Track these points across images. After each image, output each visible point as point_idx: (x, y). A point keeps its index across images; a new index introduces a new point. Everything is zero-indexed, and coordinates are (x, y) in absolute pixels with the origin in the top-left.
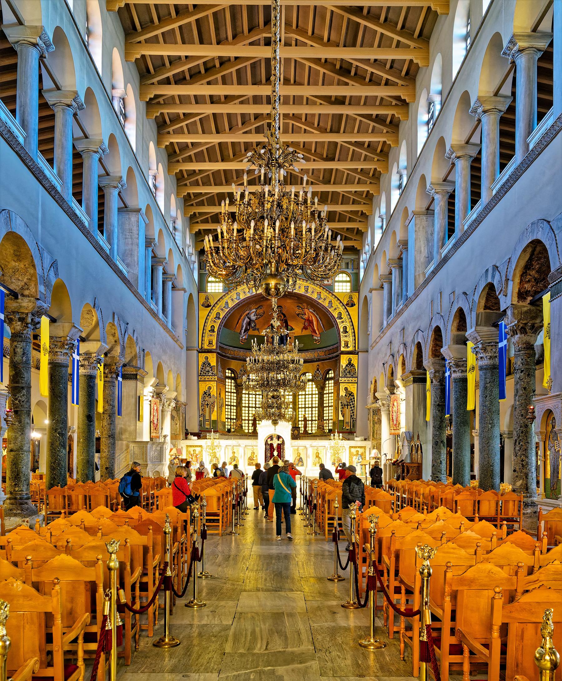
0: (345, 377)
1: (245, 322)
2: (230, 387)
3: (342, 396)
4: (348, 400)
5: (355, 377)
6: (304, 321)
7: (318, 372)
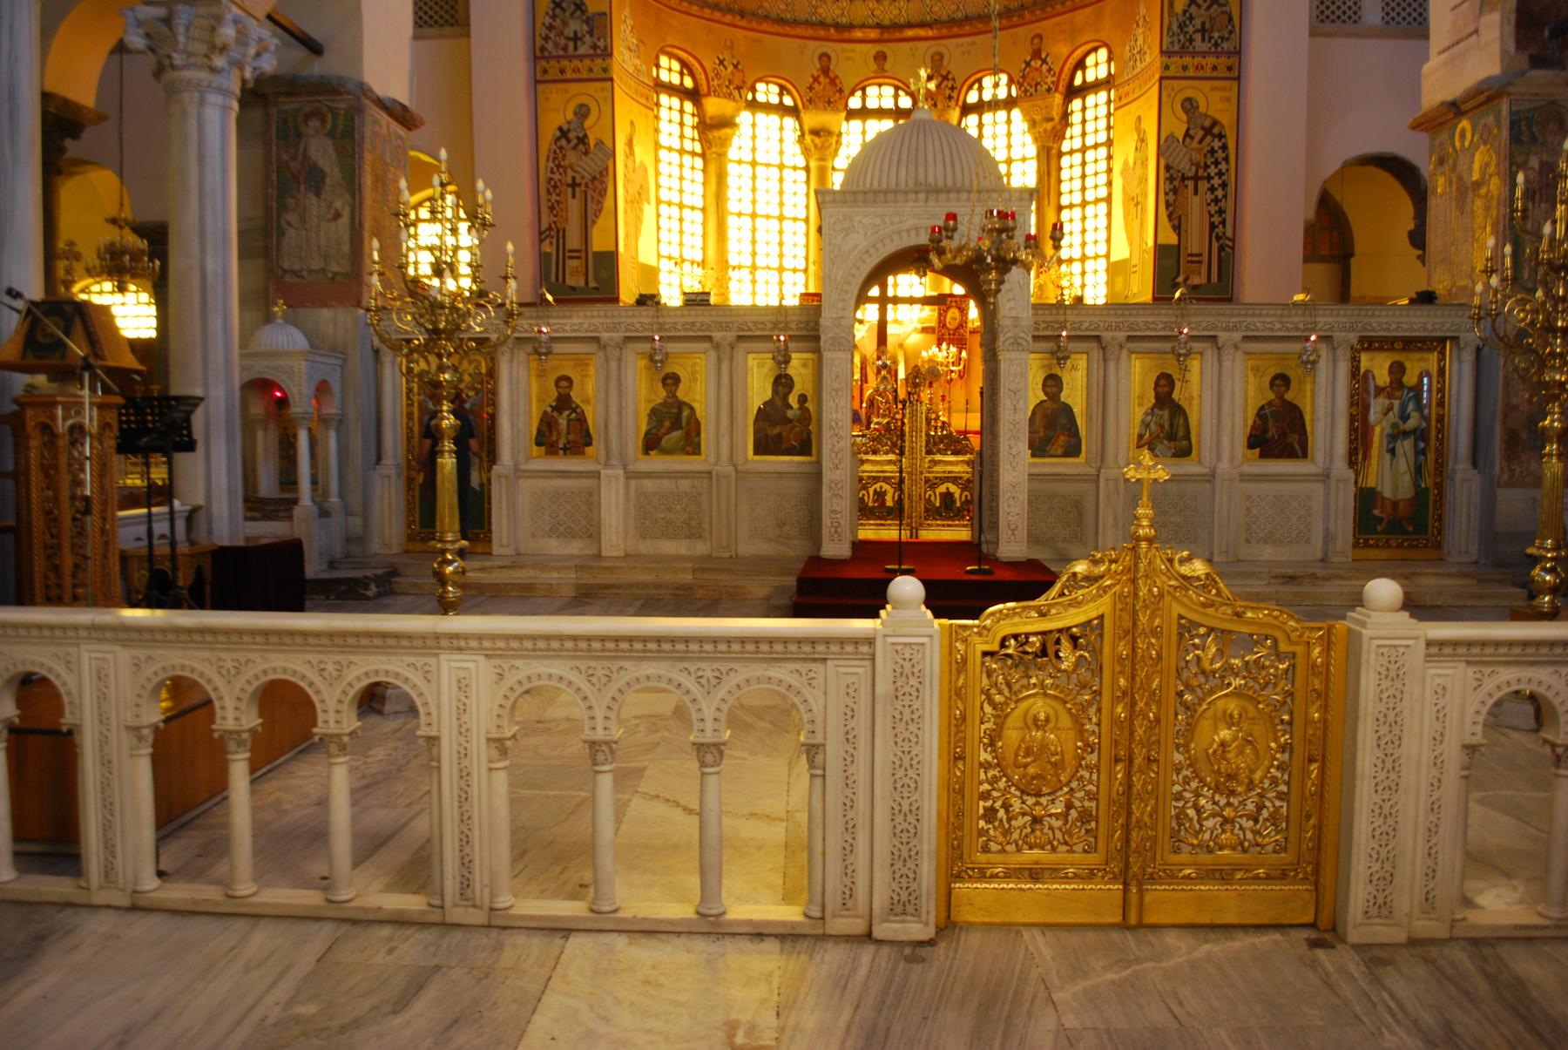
0: (1182, 52)
3: (1171, 137)
4: (1197, 157)
5: (1229, 54)
7: (1036, 64)
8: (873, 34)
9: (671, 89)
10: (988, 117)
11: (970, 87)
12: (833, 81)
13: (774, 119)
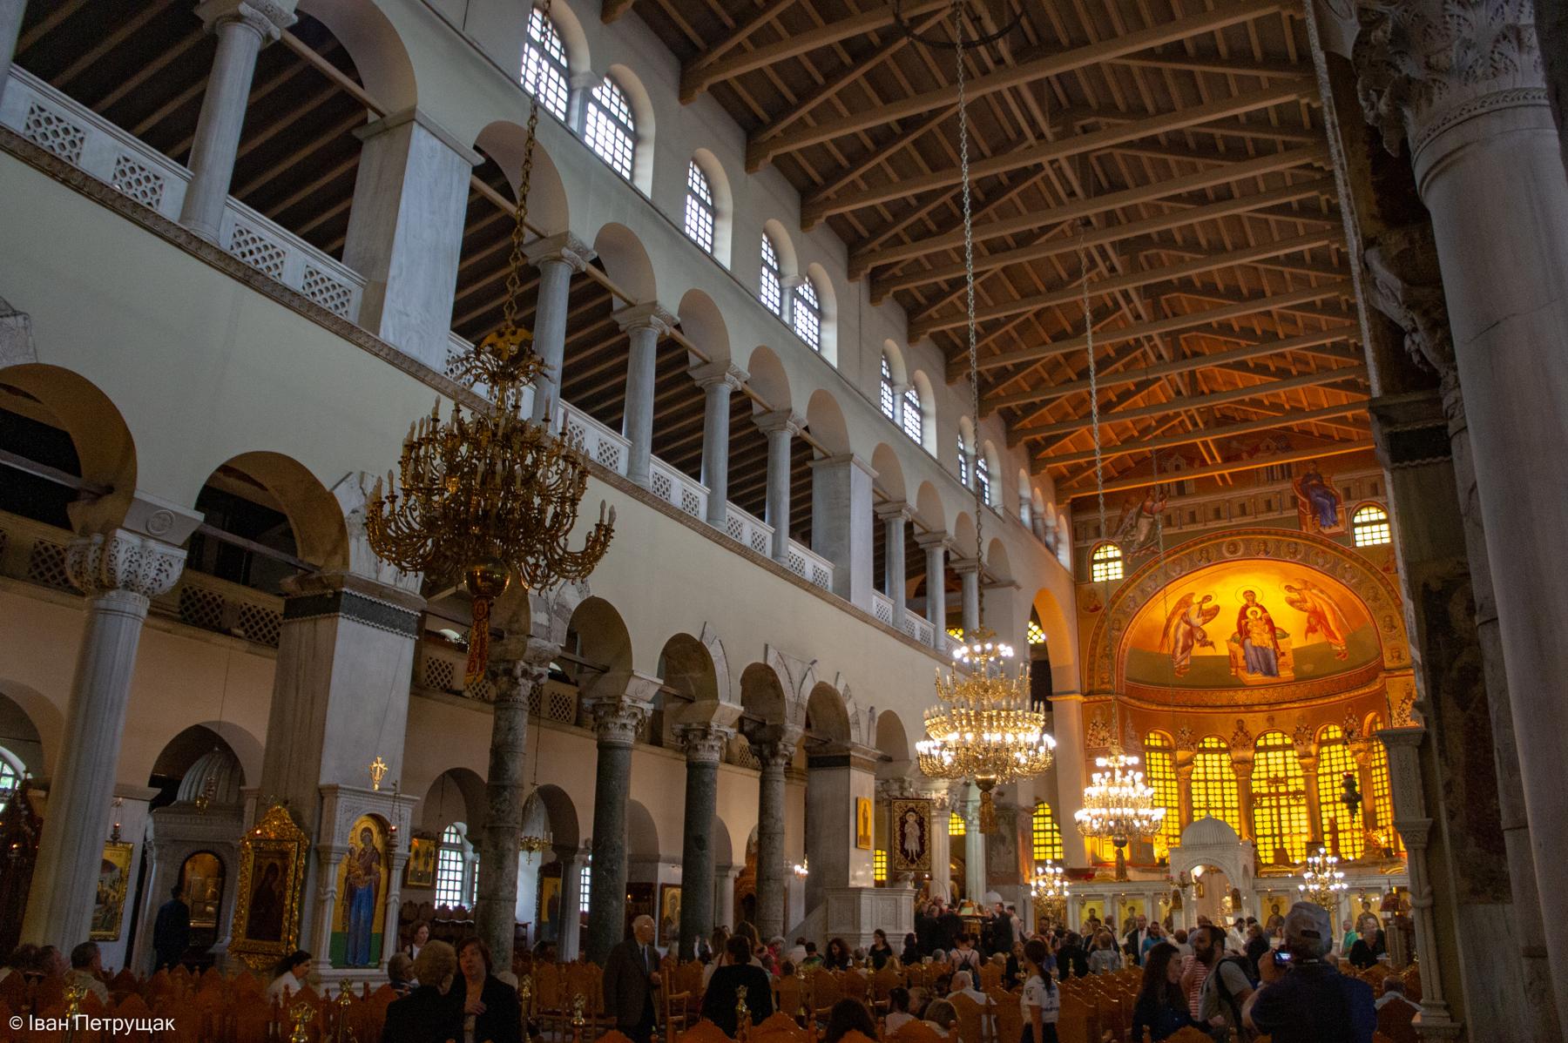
1: (1181, 631)
2: (1161, 769)
6: (1306, 614)
7: (1351, 721)
8: (1265, 708)
9: (1156, 749)
10: (1333, 748)
11: (1322, 732)
12: (1246, 734)
13: (1216, 757)
